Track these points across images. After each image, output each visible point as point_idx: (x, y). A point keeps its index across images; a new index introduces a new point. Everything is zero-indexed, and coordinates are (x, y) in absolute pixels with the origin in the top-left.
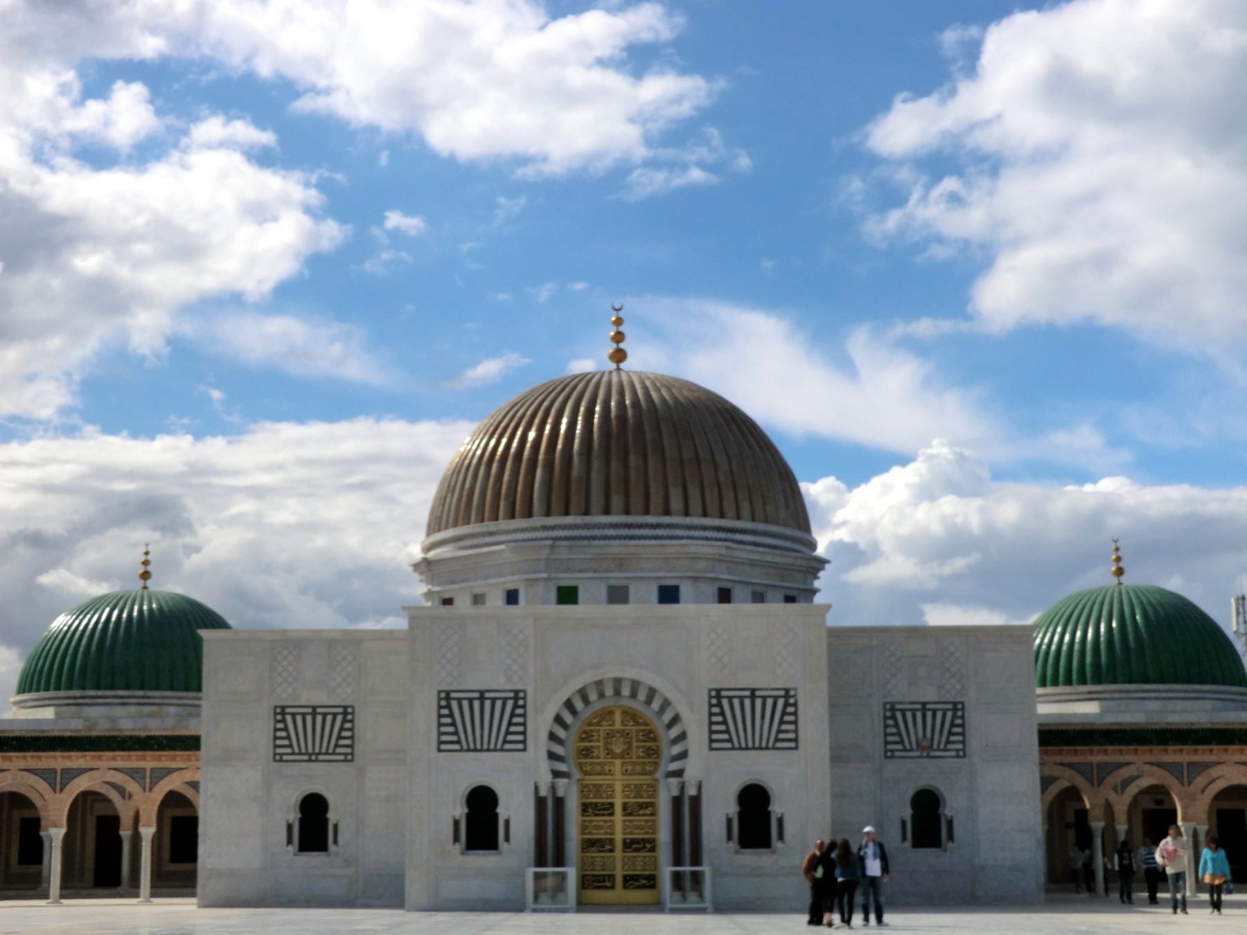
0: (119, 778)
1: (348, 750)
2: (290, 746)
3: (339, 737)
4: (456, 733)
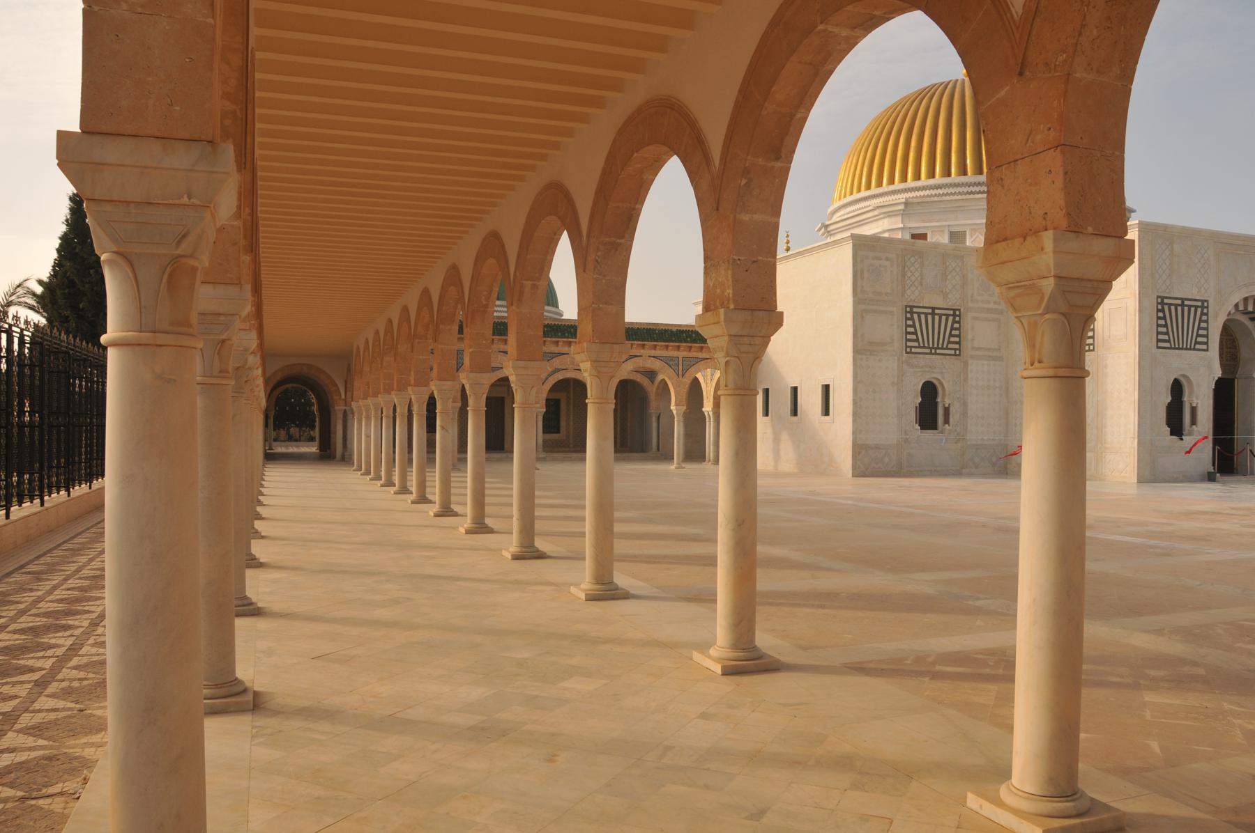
0: (655, 365)
1: (957, 346)
2: (917, 340)
3: (951, 335)
4: (1167, 333)
